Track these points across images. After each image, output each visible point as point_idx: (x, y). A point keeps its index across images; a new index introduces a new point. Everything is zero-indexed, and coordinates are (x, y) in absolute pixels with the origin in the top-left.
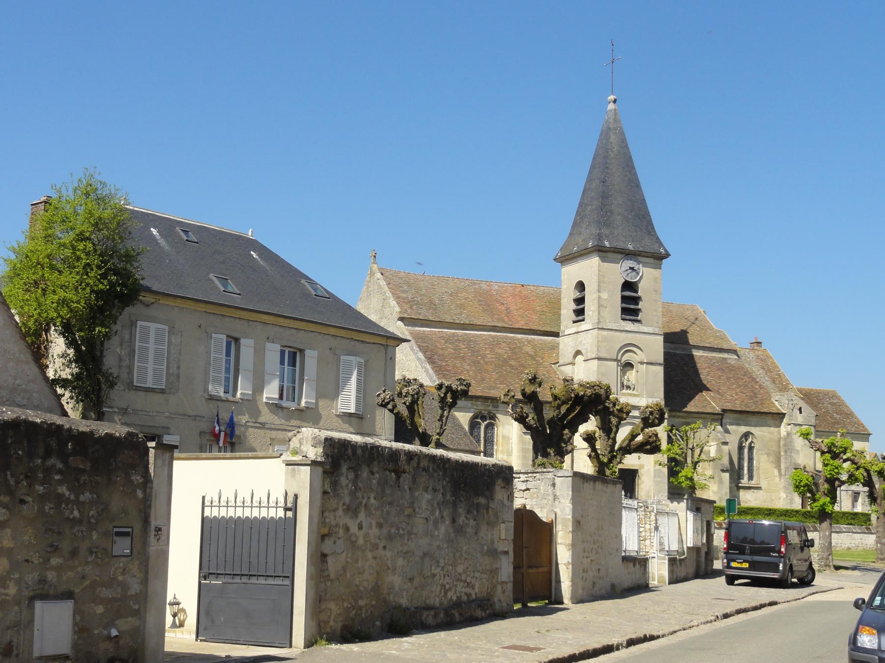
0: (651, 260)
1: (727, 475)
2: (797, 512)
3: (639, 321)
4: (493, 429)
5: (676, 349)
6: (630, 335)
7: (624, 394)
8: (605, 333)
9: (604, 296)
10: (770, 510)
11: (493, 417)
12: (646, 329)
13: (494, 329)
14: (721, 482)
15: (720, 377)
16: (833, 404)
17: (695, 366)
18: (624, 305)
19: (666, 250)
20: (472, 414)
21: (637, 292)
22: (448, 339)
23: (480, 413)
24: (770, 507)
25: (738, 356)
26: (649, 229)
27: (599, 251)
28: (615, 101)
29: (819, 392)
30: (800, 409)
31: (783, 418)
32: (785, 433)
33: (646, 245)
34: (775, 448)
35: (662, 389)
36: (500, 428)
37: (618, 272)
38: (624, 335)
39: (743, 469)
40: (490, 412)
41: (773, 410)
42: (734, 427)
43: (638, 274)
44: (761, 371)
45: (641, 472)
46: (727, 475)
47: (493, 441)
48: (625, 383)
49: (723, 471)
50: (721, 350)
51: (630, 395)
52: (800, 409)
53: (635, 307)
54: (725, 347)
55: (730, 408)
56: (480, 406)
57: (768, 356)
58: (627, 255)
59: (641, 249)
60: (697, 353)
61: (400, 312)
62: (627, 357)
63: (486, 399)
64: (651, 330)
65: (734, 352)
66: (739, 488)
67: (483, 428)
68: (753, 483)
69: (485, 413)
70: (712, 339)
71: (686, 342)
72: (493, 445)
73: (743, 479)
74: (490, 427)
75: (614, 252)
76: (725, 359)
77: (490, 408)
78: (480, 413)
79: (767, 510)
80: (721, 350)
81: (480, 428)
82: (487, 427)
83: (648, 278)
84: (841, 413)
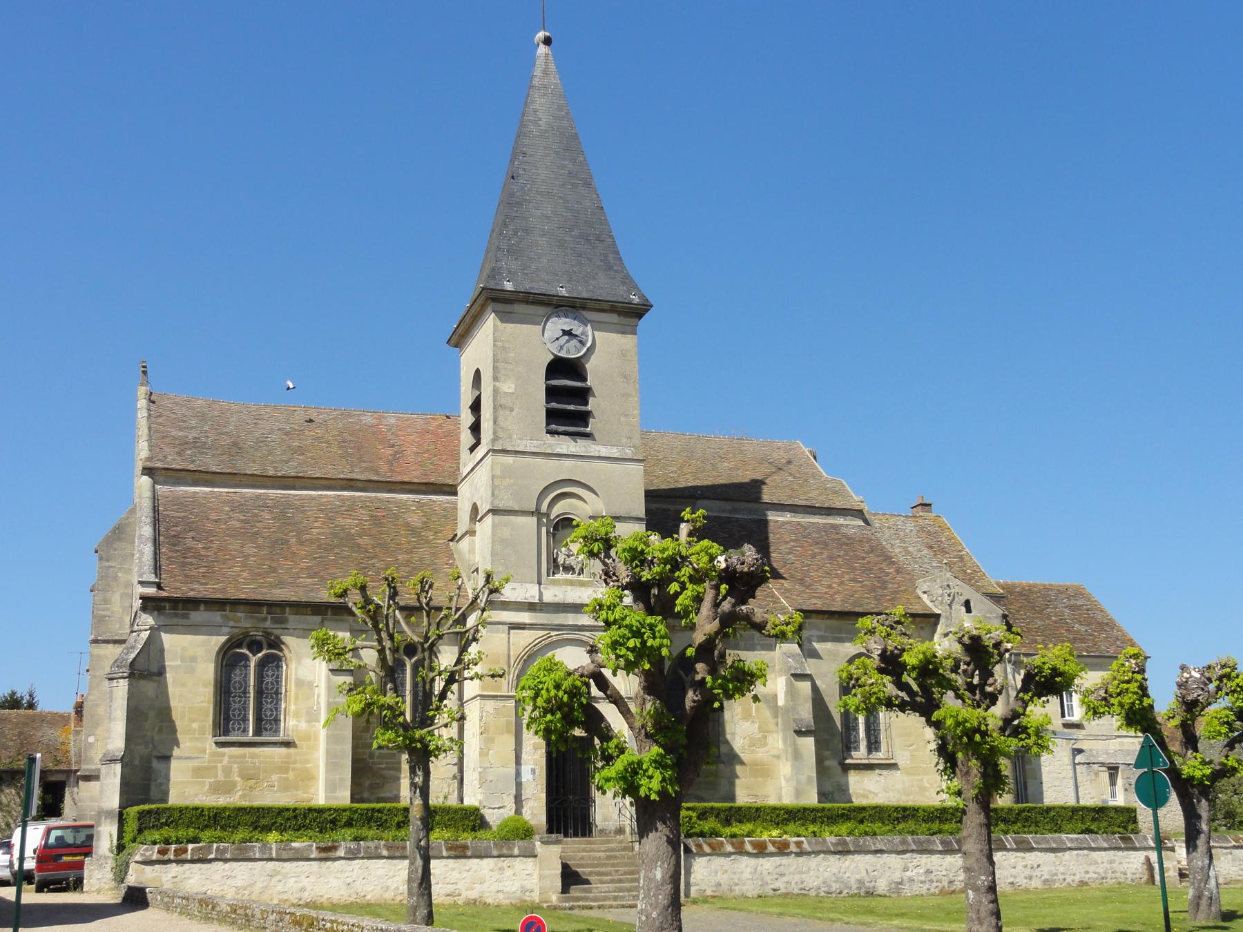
0: (614, 318)
1: (809, 742)
2: (814, 810)
4: (279, 667)
5: (735, 511)
6: (567, 463)
7: (555, 583)
8: (509, 460)
9: (508, 387)
10: (905, 809)
11: (276, 644)
12: (604, 451)
13: (350, 484)
14: (797, 755)
15: (814, 556)
16: (1074, 608)
17: (767, 538)
18: (554, 405)
19: (642, 297)
20: (223, 639)
21: (584, 379)
22: (237, 506)
23: (246, 635)
24: (903, 804)
25: (866, 521)
26: (612, 262)
27: (495, 300)
28: (547, 41)
29: (1048, 589)
30: (967, 604)
31: (936, 623)
33: (602, 287)
36: (293, 666)
37: (544, 339)
38: (552, 463)
39: (856, 729)
40: (267, 634)
41: (917, 609)
42: (829, 645)
43: (582, 343)
44: (925, 552)
46: (809, 742)
47: (278, 693)
48: (561, 560)
49: (799, 733)
50: (830, 511)
51: (571, 583)
52: (967, 604)
53: (582, 408)
54: (838, 504)
55: (818, 604)
56: (244, 621)
57: (943, 528)
58: (557, 306)
59: (585, 295)
60: (772, 516)
61: (149, 459)
62: (560, 508)
63: (254, 605)
64: (614, 452)
65: (859, 513)
66: (846, 768)
67: (252, 665)
68: (879, 757)
69: (258, 635)
70: (813, 494)
71: (757, 498)
72: (278, 701)
73: (857, 749)
74: (273, 663)
75: (527, 302)
76: (834, 527)
77: (268, 624)
78: (246, 635)
79: (896, 809)
80: (830, 511)
81: (247, 666)
82: (262, 665)
83: (609, 355)
84: (1090, 621)
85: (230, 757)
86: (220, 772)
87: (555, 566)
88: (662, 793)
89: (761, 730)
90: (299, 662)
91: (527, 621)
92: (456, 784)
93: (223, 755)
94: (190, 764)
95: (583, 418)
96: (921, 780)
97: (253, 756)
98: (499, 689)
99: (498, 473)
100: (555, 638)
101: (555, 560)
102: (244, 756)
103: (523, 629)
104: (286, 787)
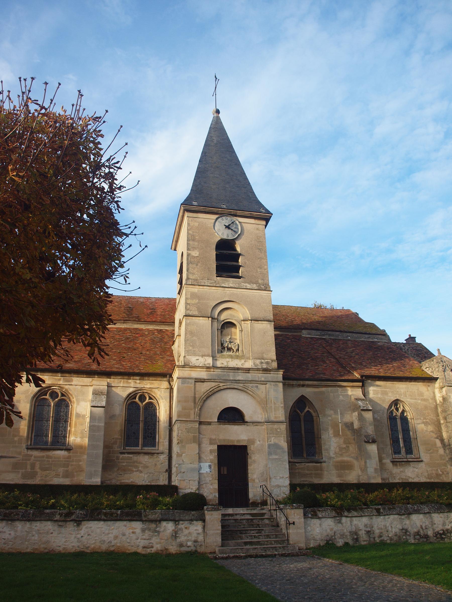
3: (239, 277)
7: (223, 357)
32: (441, 399)
34: (432, 416)
35: (274, 349)
43: (236, 232)
45: (251, 449)
51: (231, 357)
77: (61, 382)
85: (35, 457)
86: (29, 467)
87: (223, 348)
88: (52, 260)
89: (345, 442)
90: (78, 404)
91: (205, 377)
92: (166, 475)
93: (31, 456)
94: (12, 460)
95: (237, 269)
96: (437, 470)
97: (48, 457)
98: (189, 416)
99: (189, 296)
100: (222, 388)
101: (222, 344)
102: (43, 457)
103: (203, 382)
104: (66, 475)
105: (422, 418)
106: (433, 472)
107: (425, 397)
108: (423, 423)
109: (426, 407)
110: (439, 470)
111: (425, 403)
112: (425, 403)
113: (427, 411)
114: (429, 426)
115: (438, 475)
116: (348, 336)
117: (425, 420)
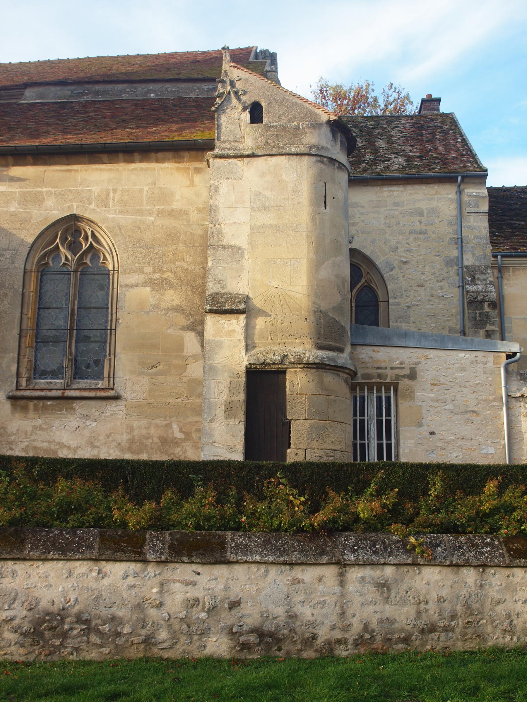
96: (169, 426)
105: (149, 270)
106: (152, 431)
107: (176, 205)
108: (150, 282)
109: (172, 237)
110: (175, 427)
111: (168, 222)
112: (168, 222)
113: (171, 248)
114: (171, 292)
115: (166, 442)
116: (149, 91)
117: (157, 275)
